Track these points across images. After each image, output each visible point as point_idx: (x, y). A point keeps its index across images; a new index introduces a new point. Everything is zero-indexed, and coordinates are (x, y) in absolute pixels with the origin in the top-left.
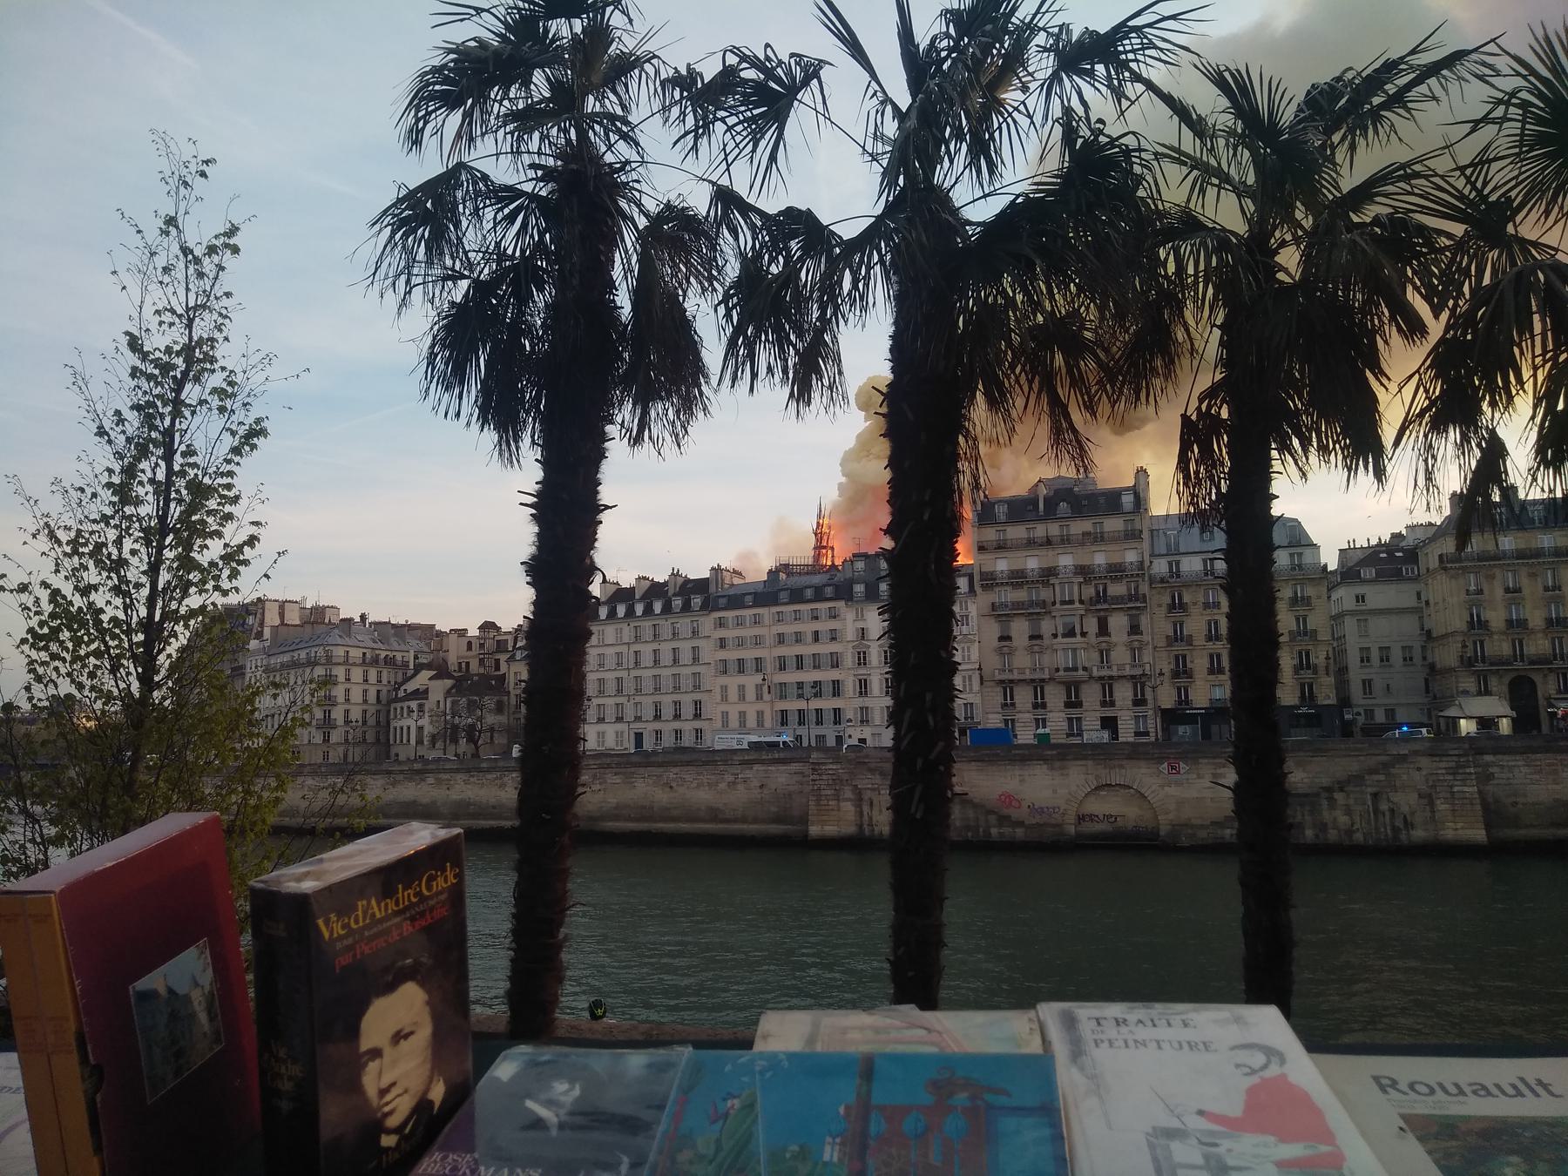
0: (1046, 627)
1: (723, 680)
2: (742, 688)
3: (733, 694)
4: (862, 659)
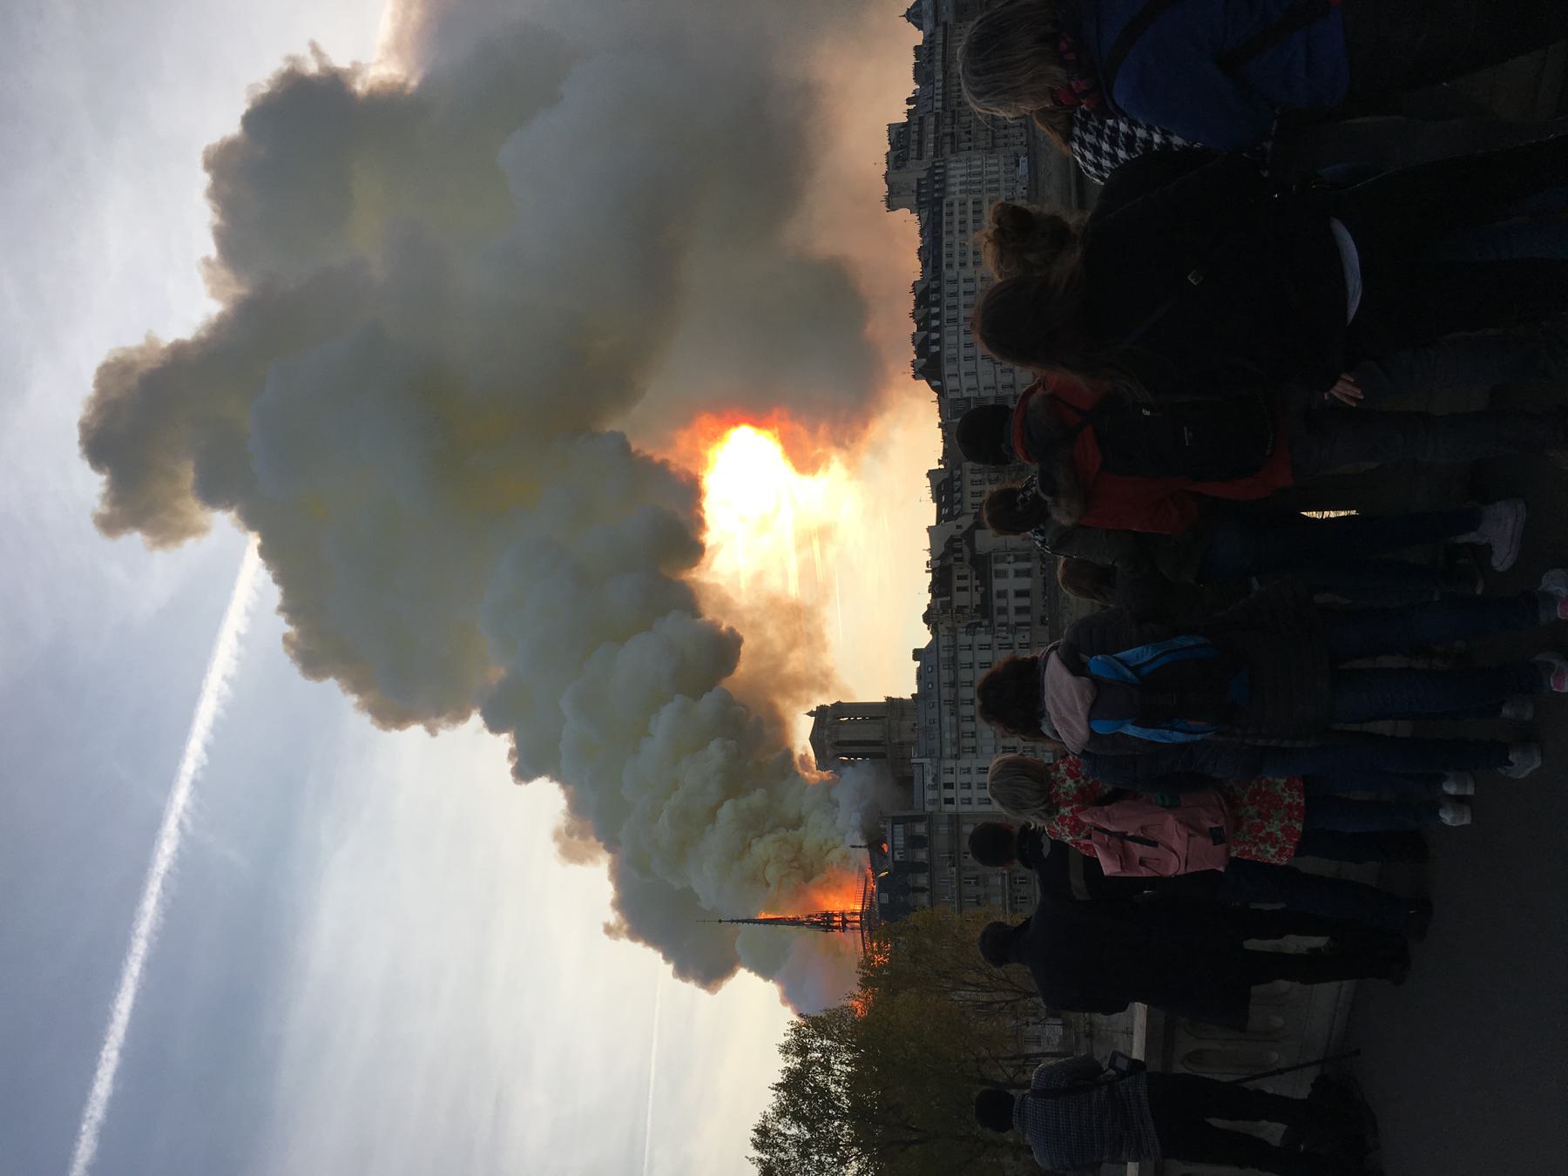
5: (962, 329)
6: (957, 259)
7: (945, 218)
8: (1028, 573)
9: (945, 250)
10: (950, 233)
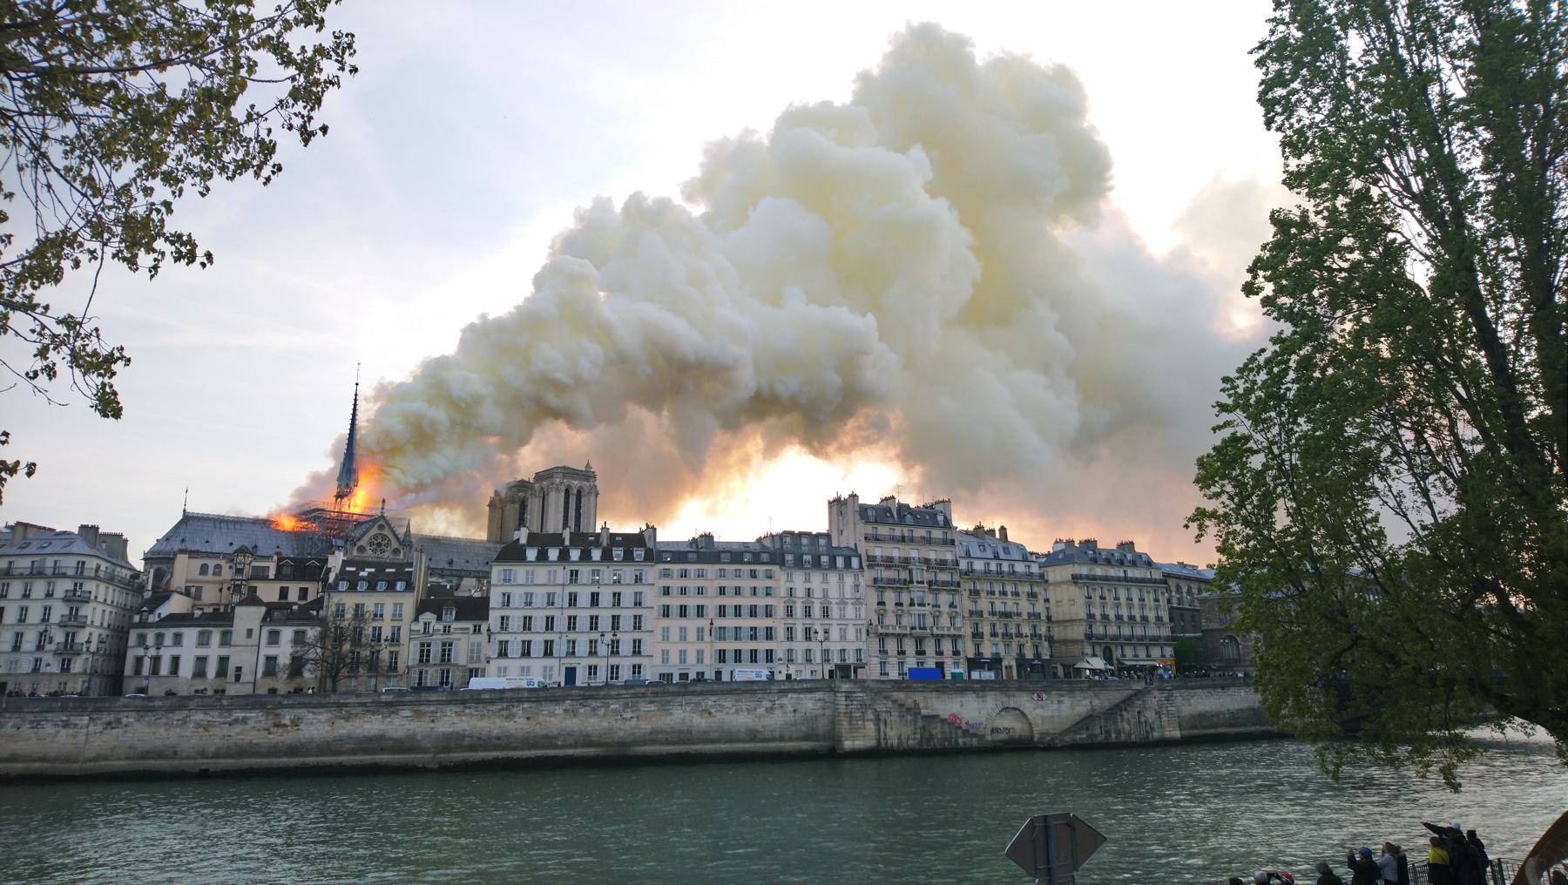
0: (905, 598)
1: (666, 622)
2: (683, 630)
3: (674, 635)
4: (790, 612)
6: (676, 584)
7: (746, 568)
8: (200, 673)
9: (692, 568)
10: (722, 574)
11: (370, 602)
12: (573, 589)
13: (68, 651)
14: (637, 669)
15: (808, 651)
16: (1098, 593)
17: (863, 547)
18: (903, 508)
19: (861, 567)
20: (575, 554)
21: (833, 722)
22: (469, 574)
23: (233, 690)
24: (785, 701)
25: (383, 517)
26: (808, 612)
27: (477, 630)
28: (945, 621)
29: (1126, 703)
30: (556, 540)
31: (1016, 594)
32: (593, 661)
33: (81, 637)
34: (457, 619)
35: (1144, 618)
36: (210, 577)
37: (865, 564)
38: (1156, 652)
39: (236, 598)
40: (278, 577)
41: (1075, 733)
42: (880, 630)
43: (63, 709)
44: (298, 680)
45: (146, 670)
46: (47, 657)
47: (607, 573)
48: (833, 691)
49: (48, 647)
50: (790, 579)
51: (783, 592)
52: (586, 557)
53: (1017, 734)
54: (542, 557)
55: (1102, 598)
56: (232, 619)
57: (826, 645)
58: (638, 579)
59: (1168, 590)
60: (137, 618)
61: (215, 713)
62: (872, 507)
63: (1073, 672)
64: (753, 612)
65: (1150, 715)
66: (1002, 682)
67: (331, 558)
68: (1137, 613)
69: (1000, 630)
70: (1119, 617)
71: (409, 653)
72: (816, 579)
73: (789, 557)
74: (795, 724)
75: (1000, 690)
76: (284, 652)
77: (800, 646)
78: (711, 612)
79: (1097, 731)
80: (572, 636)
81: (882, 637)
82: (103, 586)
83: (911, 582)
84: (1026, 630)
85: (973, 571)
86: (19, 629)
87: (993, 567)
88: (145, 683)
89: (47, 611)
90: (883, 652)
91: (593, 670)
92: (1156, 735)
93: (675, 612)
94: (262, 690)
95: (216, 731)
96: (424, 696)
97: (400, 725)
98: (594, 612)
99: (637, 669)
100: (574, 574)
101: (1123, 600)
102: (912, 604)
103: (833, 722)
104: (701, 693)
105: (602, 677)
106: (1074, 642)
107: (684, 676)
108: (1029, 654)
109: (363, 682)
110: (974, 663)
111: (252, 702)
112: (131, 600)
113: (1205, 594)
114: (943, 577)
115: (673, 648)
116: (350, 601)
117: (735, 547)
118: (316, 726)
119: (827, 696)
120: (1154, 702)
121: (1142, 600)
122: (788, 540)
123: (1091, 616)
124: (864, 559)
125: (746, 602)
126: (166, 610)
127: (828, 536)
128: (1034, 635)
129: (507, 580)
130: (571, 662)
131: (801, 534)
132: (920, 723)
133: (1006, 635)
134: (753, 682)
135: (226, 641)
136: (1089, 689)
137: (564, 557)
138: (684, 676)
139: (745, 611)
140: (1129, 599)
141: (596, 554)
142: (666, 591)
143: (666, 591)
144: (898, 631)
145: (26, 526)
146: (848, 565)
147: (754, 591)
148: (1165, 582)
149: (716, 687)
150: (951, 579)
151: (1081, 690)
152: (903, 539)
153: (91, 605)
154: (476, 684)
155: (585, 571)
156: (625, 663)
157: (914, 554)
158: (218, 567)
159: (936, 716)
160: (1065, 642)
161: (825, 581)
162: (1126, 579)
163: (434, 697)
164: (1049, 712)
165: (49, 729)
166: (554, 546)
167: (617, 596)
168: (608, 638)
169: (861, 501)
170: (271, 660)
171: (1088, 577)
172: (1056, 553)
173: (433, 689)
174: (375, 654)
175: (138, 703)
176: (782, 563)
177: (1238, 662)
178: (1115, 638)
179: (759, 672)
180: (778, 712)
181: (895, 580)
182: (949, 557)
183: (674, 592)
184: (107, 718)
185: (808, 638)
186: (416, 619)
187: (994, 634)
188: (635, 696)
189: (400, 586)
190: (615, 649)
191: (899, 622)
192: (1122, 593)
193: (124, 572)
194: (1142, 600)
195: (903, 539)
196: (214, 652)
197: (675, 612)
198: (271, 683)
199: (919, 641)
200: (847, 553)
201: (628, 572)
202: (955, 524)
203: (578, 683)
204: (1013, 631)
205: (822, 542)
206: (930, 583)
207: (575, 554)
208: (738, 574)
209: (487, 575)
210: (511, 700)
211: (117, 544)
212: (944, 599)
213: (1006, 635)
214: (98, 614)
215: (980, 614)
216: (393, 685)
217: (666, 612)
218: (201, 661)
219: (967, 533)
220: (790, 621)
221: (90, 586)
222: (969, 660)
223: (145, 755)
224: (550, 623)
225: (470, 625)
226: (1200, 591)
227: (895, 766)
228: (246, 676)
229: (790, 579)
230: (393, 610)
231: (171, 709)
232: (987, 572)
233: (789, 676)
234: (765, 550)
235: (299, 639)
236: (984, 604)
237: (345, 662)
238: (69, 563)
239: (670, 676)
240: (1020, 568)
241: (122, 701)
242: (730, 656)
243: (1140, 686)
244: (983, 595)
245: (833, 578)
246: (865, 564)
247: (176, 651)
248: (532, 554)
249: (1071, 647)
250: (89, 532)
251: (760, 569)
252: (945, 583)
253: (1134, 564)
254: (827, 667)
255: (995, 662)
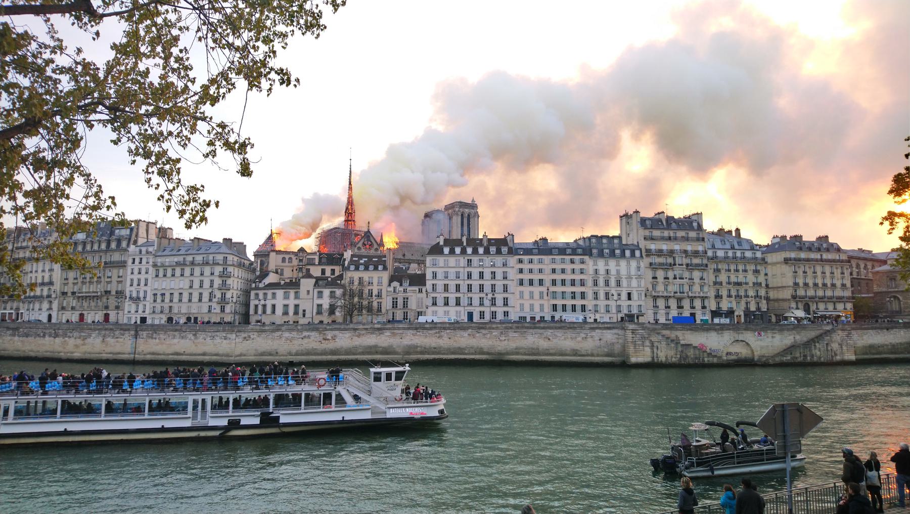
1: (521, 288)
2: (531, 293)
4: (596, 283)
5: (461, 270)
6: (526, 266)
7: (568, 258)
8: (286, 313)
9: (536, 258)
10: (553, 261)
11: (366, 276)
12: (469, 269)
13: (223, 301)
14: (506, 314)
15: (607, 306)
16: (802, 269)
17: (643, 244)
18: (670, 219)
19: (641, 256)
20: (469, 250)
21: (624, 347)
22: (414, 261)
23: (302, 321)
24: (594, 334)
25: (369, 231)
26: (607, 283)
27: (420, 291)
28: (696, 288)
29: (819, 338)
30: (459, 242)
31: (745, 271)
32: (482, 309)
33: (229, 295)
34: (410, 285)
35: (833, 285)
36: (287, 264)
37: (644, 254)
38: (840, 306)
39: (300, 275)
40: (320, 263)
41: (783, 356)
42: (654, 294)
43: (224, 331)
44: (333, 316)
45: (260, 312)
46: (214, 305)
47: (487, 260)
48: (623, 329)
49: (214, 300)
50: (595, 264)
51: (591, 271)
52: (475, 252)
53: (743, 356)
54: (452, 252)
55: (805, 272)
56: (299, 285)
57: (619, 303)
58: (505, 265)
59: (851, 267)
60: (253, 285)
61: (295, 333)
62: (649, 219)
63: (781, 317)
64: (573, 283)
65: (835, 346)
66: (734, 325)
67: (345, 253)
68: (828, 282)
69: (733, 293)
70: (816, 285)
71: (387, 303)
72: (612, 264)
73: (595, 251)
74: (600, 347)
75: (734, 330)
76: (326, 302)
77: (602, 303)
78: (548, 283)
79: (798, 355)
80: (470, 295)
81: (655, 298)
82: (236, 269)
83: (675, 264)
84: (751, 293)
85: (716, 257)
86: (201, 291)
87: (730, 254)
88: (259, 318)
89: (212, 282)
90: (656, 307)
91: (482, 315)
92: (838, 358)
93: (526, 282)
94: (316, 322)
95: (295, 342)
96: (396, 325)
97: (384, 340)
98: (481, 282)
99: (506, 314)
100: (469, 261)
101: (819, 274)
102: (675, 278)
103: (624, 347)
104: (543, 328)
105: (487, 317)
106: (784, 300)
107: (533, 318)
108: (753, 308)
109: (365, 317)
110: (716, 314)
111: (311, 327)
112: (250, 276)
113: (877, 269)
114: (696, 261)
115: (527, 302)
116: (356, 275)
117: (561, 246)
118: (344, 341)
119: (620, 332)
120: (838, 338)
121: (832, 273)
122: (594, 240)
123: (796, 284)
124: (644, 251)
125: (568, 277)
126: (267, 281)
127: (619, 237)
128: (757, 296)
129: (434, 265)
130: (470, 309)
131: (602, 237)
132: (680, 349)
133: (738, 296)
134: (574, 323)
135: (297, 297)
136: (793, 329)
137: (464, 252)
138: (533, 318)
139: (568, 283)
140: (823, 273)
141: (481, 250)
142: (521, 271)
143: (521, 271)
144: (665, 294)
145: (199, 239)
146: (633, 255)
147: (573, 271)
148: (849, 262)
149: (552, 325)
150: (700, 262)
151: (788, 330)
152: (670, 238)
153: (232, 279)
154: (422, 319)
155: (475, 259)
156: (500, 311)
157: (677, 247)
158: (290, 258)
159: (691, 345)
160: (777, 300)
161: (618, 265)
162: (822, 260)
163: (401, 326)
164: (765, 343)
165: (218, 340)
166: (458, 246)
167: (493, 273)
168: (490, 296)
169: (642, 215)
170: (320, 306)
171: (795, 259)
172: (773, 244)
173: (400, 322)
174: (370, 303)
175: (258, 328)
176: (591, 255)
177: (899, 313)
178: (811, 298)
179: (578, 317)
180: (590, 340)
181: (664, 263)
182: (700, 248)
183: (526, 271)
184: (244, 335)
185: (607, 298)
186: (390, 285)
187: (729, 296)
188: (506, 328)
189: (380, 267)
190: (493, 302)
191: (666, 289)
192: (819, 269)
193: (246, 262)
194: (832, 273)
195: (670, 238)
196: (292, 302)
197: (526, 282)
198: (320, 318)
199: (679, 300)
200: (632, 247)
201: (499, 260)
202: (705, 227)
203: (475, 320)
204: (742, 293)
205: (616, 241)
206: (687, 265)
207: (469, 250)
208: (563, 261)
209: (424, 262)
210: (440, 328)
211: (240, 248)
212: (696, 274)
213: (738, 296)
214: (236, 283)
215: (721, 283)
216: (381, 319)
217: (521, 283)
218: (286, 306)
219: (713, 233)
220: (596, 288)
221: (230, 269)
222: (712, 312)
223: (262, 354)
224: (458, 288)
225: (417, 288)
226: (873, 267)
227: (663, 373)
228: (308, 315)
229: (595, 264)
230: (378, 280)
231: (273, 331)
232: (726, 258)
233: (595, 320)
234: (579, 247)
235: (332, 295)
236: (723, 278)
237: (355, 308)
238: (220, 258)
239: (525, 318)
240: (748, 254)
241: (250, 327)
242: (559, 308)
243: (829, 328)
244: (723, 272)
245: (623, 263)
246: (644, 254)
247: (273, 302)
248: (446, 250)
249: (781, 303)
250: (227, 241)
251: (577, 258)
252: (697, 265)
253: (828, 250)
254: (620, 315)
255: (730, 313)
